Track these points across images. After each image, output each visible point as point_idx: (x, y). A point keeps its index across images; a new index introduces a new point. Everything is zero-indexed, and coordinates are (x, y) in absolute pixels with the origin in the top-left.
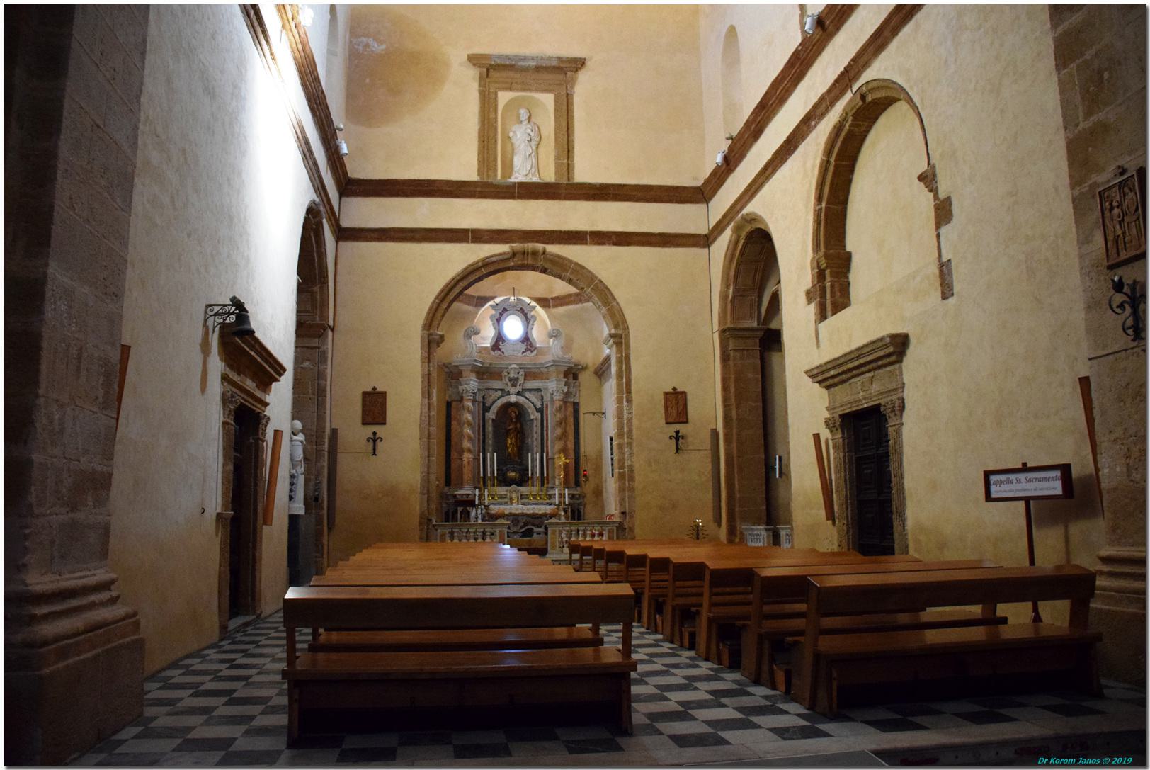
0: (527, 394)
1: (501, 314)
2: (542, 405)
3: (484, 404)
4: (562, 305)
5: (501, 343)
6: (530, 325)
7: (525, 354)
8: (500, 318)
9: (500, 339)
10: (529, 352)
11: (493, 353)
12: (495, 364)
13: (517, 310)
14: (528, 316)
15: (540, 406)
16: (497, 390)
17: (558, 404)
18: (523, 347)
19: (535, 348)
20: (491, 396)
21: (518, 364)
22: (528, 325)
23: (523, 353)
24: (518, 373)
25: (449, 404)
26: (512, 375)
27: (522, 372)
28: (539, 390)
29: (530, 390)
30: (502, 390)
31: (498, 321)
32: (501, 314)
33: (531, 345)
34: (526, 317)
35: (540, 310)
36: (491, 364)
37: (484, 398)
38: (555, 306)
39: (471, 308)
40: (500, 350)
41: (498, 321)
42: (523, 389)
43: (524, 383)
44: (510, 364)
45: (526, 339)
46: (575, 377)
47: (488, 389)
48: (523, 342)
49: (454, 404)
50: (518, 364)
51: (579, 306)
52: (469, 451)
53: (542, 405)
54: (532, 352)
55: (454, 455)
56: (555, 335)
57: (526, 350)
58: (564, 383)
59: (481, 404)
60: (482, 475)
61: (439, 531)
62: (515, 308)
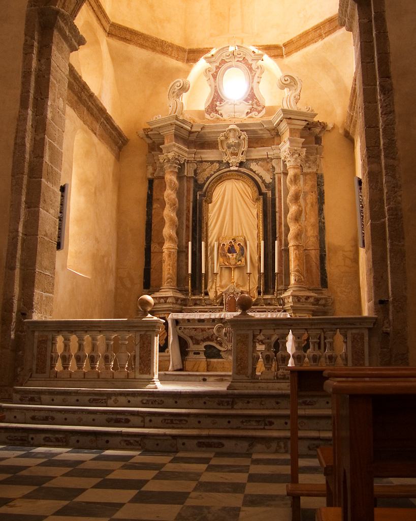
0: (254, 166)
1: (218, 68)
2: (274, 179)
3: (196, 181)
4: (297, 49)
5: (218, 103)
6: (256, 80)
7: (250, 115)
8: (217, 72)
9: (217, 98)
10: (257, 113)
11: (207, 116)
12: (208, 127)
13: (238, 61)
14: (254, 67)
15: (271, 181)
16: (212, 162)
17: (291, 173)
18: (246, 107)
19: (264, 107)
20: (204, 170)
21: (237, 125)
22: (253, 79)
23: (248, 113)
24: (239, 137)
25: (151, 182)
26: (232, 140)
27: (244, 135)
28: (267, 160)
29: (256, 160)
30: (220, 162)
31: (215, 76)
32: (218, 68)
33: (258, 104)
34: (251, 69)
35: (268, 61)
36: (203, 128)
37: (195, 171)
38: (289, 54)
39: (180, 64)
40: (217, 112)
41: (215, 75)
42: (247, 160)
43: (247, 151)
44: (228, 125)
45: (252, 97)
46: (318, 140)
47: (202, 162)
48: (246, 100)
49: (156, 182)
50: (237, 125)
51: (320, 43)
52: (171, 238)
53: (274, 179)
54: (259, 112)
55: (154, 248)
56: (289, 82)
57: (252, 110)
58: (301, 145)
59: (192, 181)
60: (190, 272)
61: (36, 334)
62: (237, 59)
